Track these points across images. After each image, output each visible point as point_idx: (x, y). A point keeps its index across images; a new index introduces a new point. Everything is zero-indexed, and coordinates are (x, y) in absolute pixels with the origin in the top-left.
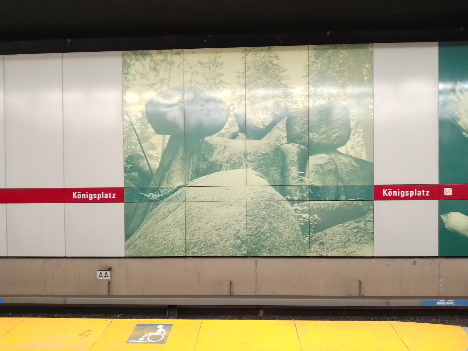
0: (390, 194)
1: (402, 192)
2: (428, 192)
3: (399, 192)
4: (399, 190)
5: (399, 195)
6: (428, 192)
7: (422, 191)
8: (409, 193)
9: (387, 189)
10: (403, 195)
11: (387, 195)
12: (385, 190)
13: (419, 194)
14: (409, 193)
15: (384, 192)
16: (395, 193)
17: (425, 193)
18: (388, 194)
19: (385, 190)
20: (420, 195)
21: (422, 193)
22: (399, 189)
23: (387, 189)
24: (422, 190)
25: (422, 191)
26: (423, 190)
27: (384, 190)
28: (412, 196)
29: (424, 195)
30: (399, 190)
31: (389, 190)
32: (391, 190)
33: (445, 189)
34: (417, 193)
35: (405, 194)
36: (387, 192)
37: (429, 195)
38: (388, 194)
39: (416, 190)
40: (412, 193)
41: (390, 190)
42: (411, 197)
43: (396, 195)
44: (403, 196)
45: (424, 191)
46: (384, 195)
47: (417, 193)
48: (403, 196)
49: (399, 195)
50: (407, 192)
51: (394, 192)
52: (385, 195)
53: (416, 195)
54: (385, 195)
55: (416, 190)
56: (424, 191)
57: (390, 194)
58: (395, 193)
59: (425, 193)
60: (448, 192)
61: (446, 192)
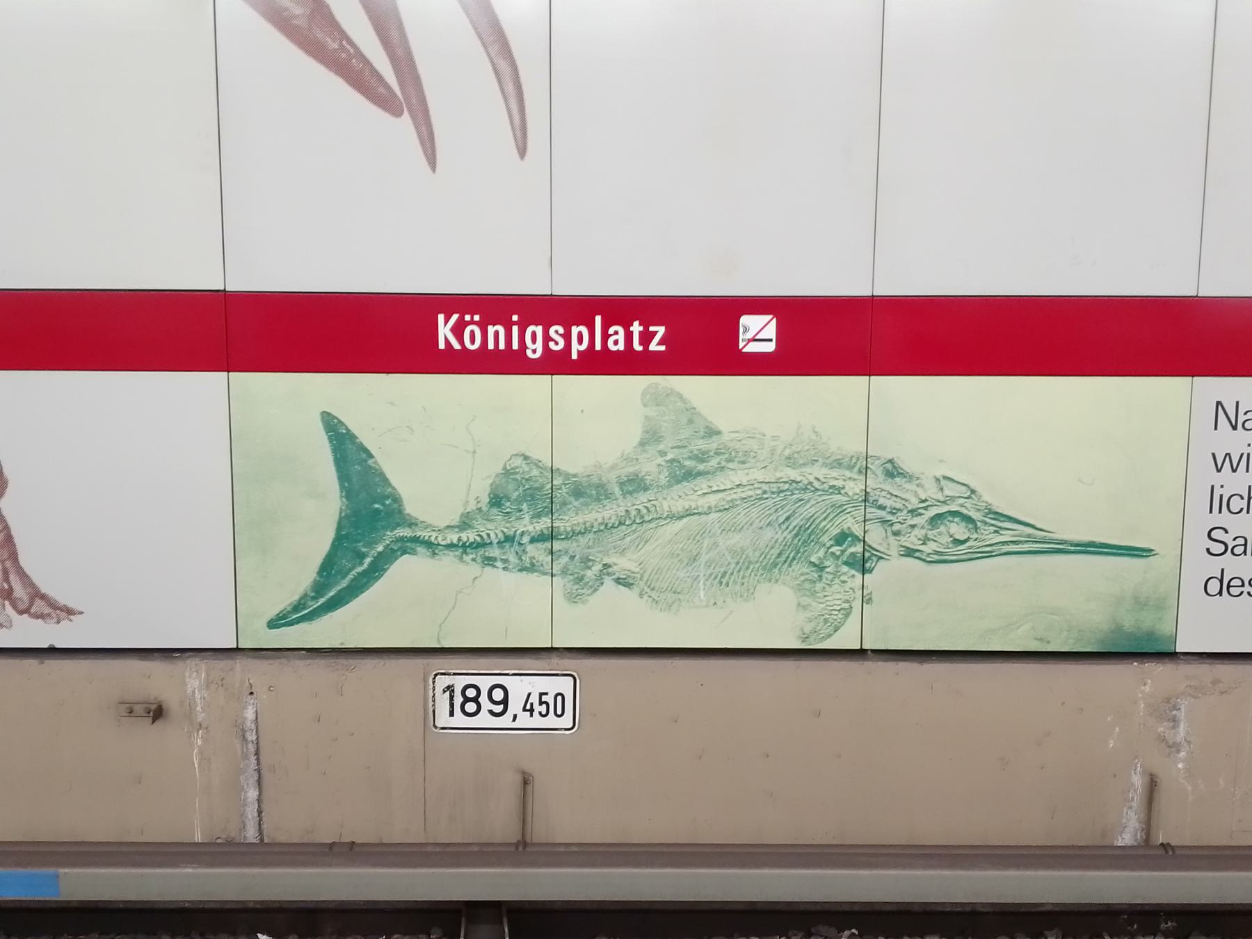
0: (473, 341)
1: (530, 329)
2: (661, 330)
3: (515, 329)
4: (515, 323)
5: (515, 346)
6: (661, 330)
7: (631, 329)
8: (567, 337)
9: (455, 317)
10: (533, 347)
11: (457, 346)
12: (446, 322)
13: (617, 341)
14: (567, 337)
15: (444, 331)
16: (496, 334)
17: (646, 338)
18: (460, 339)
19: (446, 322)
20: (621, 347)
21: (629, 337)
22: (515, 318)
23: (455, 317)
24: (632, 325)
25: (631, 329)
26: (636, 323)
27: (441, 317)
28: (579, 352)
29: (637, 347)
30: (515, 323)
31: (468, 318)
32: (477, 318)
33: (745, 320)
34: (605, 337)
35: (547, 338)
36: (458, 331)
37: (663, 348)
38: (460, 339)
39: (598, 319)
40: (580, 340)
41: (472, 322)
42: (574, 356)
43: (502, 346)
44: (535, 351)
45: (641, 328)
46: (442, 346)
47: (605, 337)
48: (535, 351)
49: (515, 346)
50: (556, 330)
51: (491, 330)
52: (447, 342)
53: (598, 347)
54: (447, 342)
55: (598, 319)
56: (641, 328)
57: (473, 341)
58: (496, 334)
59: (646, 338)
60: (757, 338)
61: (749, 335)
